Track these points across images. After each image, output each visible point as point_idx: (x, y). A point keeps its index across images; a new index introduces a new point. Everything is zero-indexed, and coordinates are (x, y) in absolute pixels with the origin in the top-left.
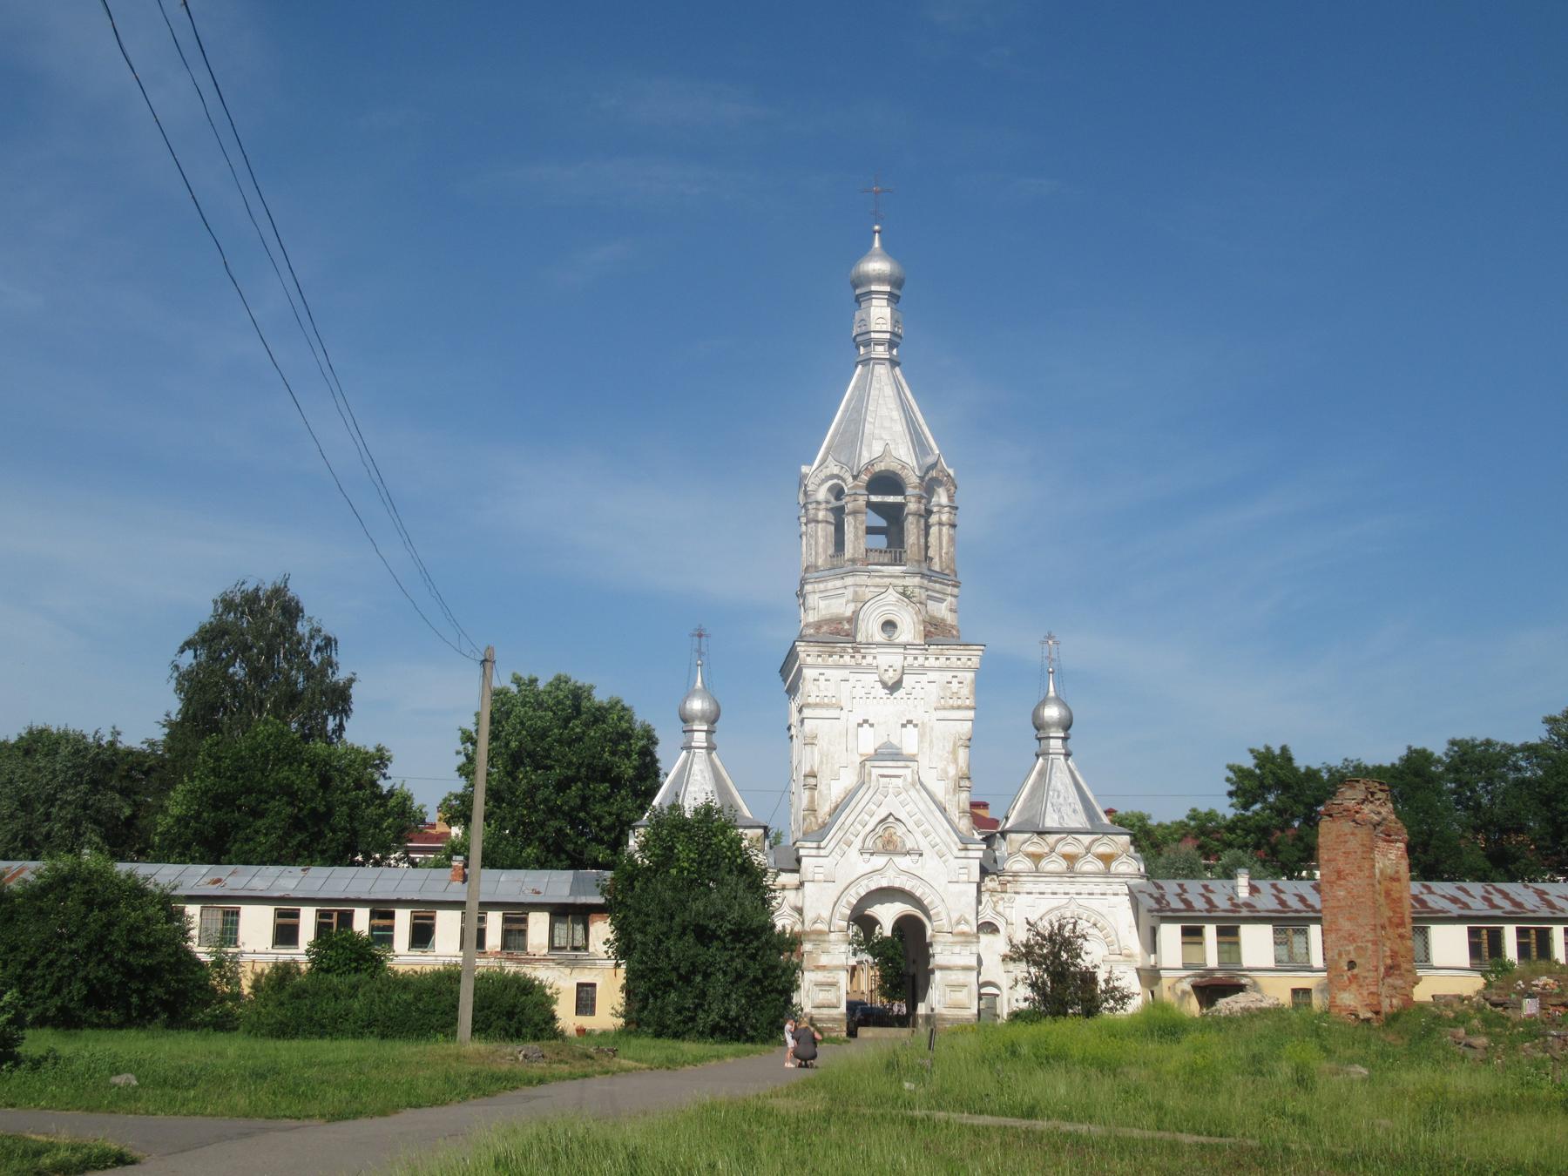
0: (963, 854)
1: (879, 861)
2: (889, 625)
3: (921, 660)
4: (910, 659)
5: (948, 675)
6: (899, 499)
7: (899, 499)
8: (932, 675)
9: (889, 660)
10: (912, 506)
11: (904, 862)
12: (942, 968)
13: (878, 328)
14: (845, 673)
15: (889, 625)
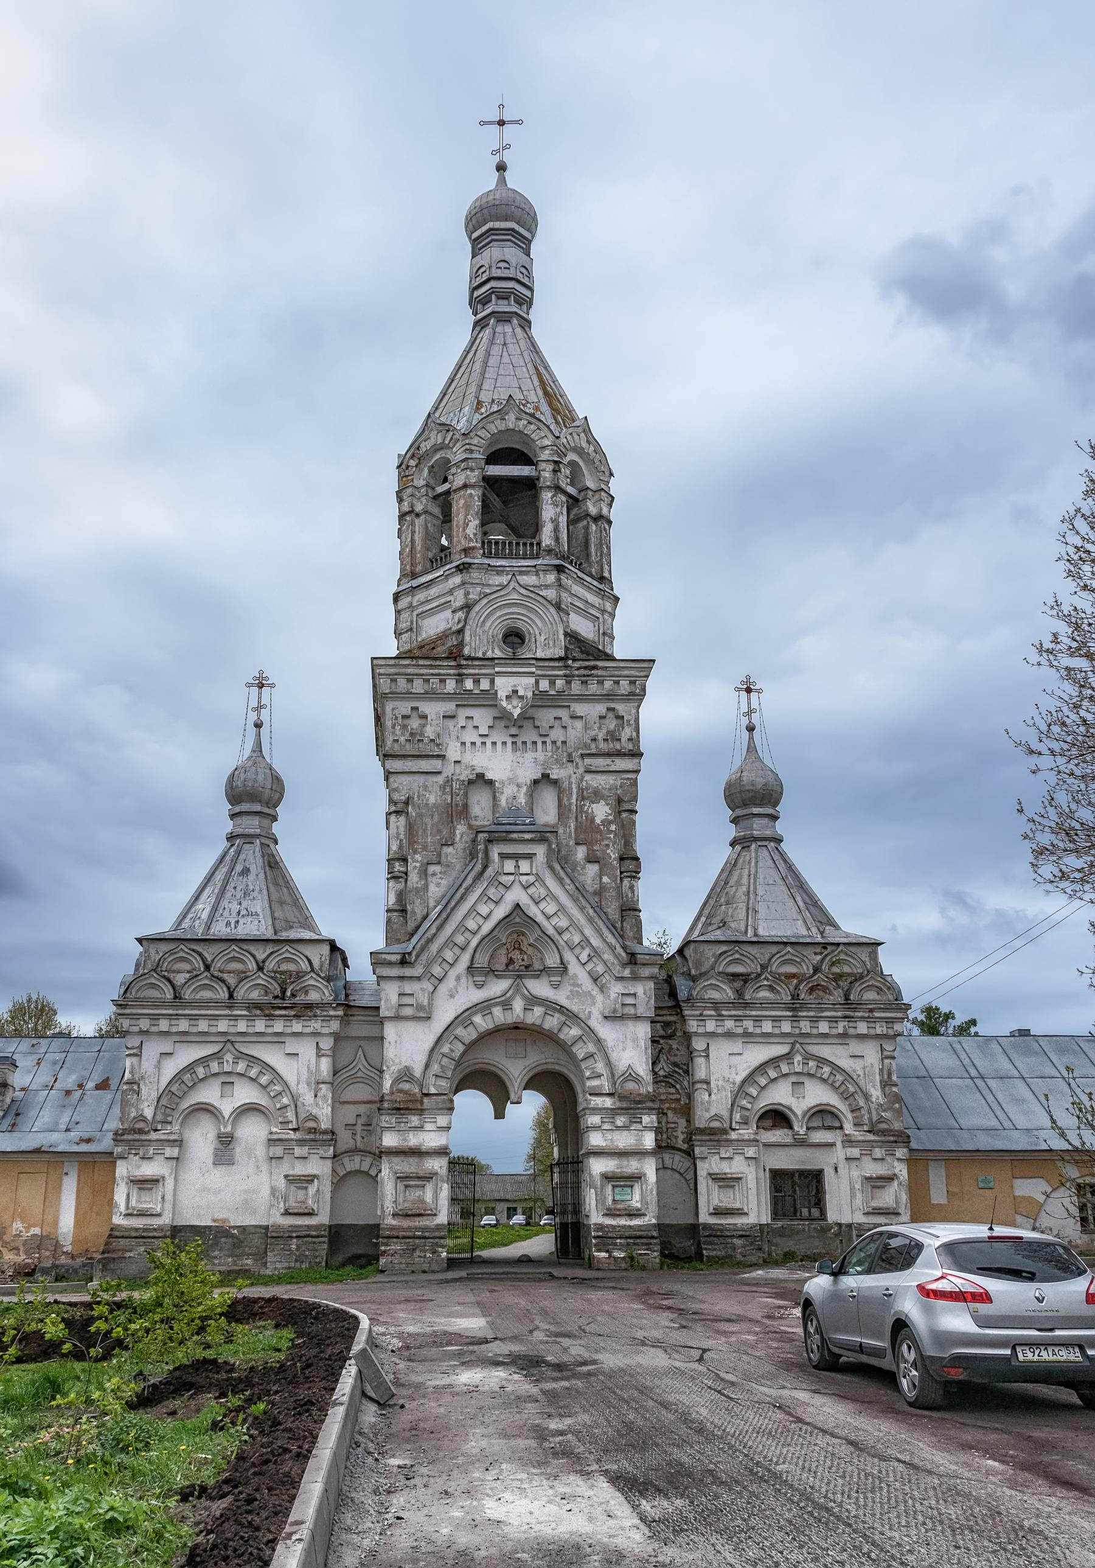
0: (627, 973)
1: (498, 987)
2: (514, 637)
3: (560, 683)
4: (544, 685)
5: (600, 708)
6: (525, 471)
7: (525, 471)
8: (580, 709)
9: (512, 685)
10: (547, 475)
11: (540, 988)
12: (599, 1153)
13: (499, 273)
14: (449, 707)
15: (514, 637)
